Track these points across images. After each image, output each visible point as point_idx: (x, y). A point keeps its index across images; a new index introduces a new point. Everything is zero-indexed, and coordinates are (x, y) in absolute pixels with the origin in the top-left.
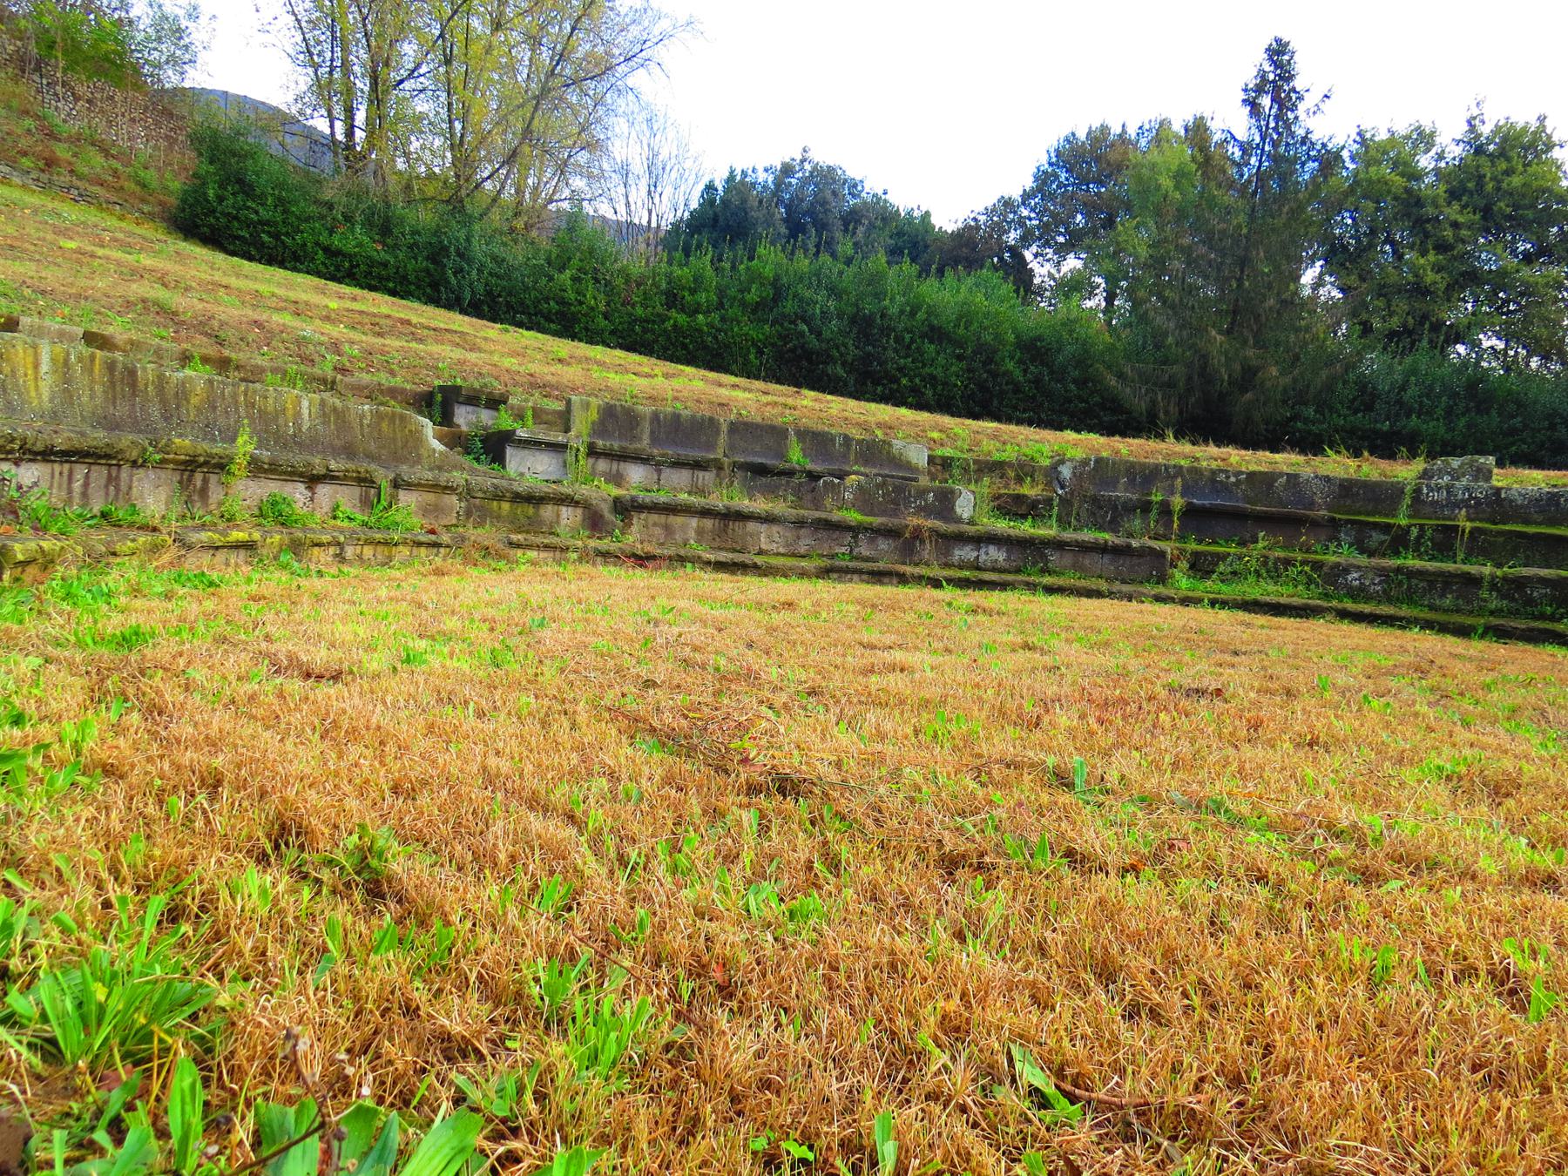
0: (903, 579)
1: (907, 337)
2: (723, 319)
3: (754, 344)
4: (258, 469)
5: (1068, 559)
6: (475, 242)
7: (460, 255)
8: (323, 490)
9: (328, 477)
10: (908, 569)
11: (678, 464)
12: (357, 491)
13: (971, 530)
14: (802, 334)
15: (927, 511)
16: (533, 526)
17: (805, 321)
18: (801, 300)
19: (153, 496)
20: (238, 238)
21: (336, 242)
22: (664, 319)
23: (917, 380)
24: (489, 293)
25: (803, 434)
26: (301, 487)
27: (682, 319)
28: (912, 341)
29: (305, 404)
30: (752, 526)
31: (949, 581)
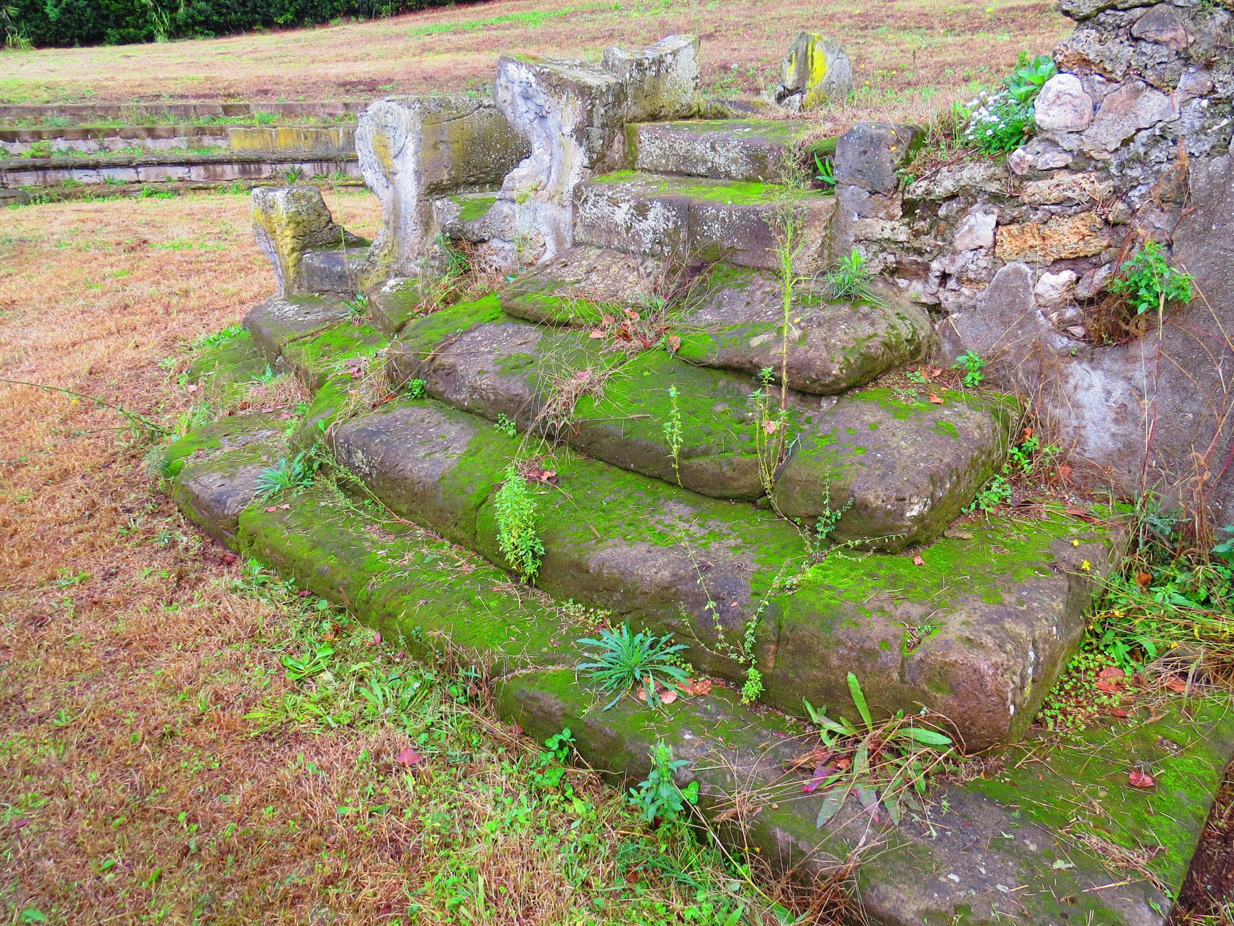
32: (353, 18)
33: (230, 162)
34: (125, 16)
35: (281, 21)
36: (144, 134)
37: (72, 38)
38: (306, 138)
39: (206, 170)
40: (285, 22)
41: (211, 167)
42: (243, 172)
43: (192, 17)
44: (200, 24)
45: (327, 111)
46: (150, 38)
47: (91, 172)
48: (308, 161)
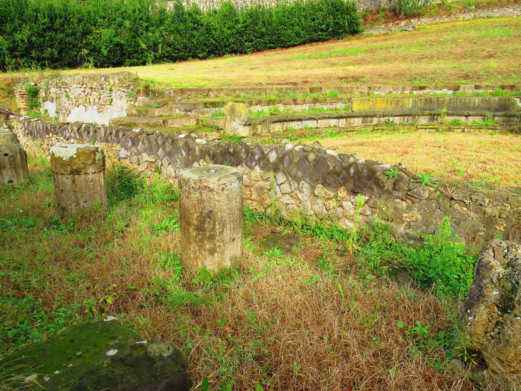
4: (448, 115)
9: (469, 115)
12: (481, 118)
19: (423, 120)
26: (464, 117)
29: (477, 100)
32: (233, 54)
33: (359, 117)
34: (133, 53)
35: (201, 55)
36: (292, 102)
37: (109, 64)
38: (391, 104)
39: (347, 121)
40: (203, 56)
41: (349, 119)
42: (363, 122)
43: (163, 54)
44: (166, 57)
45: (359, 90)
46: (144, 64)
47: (299, 123)
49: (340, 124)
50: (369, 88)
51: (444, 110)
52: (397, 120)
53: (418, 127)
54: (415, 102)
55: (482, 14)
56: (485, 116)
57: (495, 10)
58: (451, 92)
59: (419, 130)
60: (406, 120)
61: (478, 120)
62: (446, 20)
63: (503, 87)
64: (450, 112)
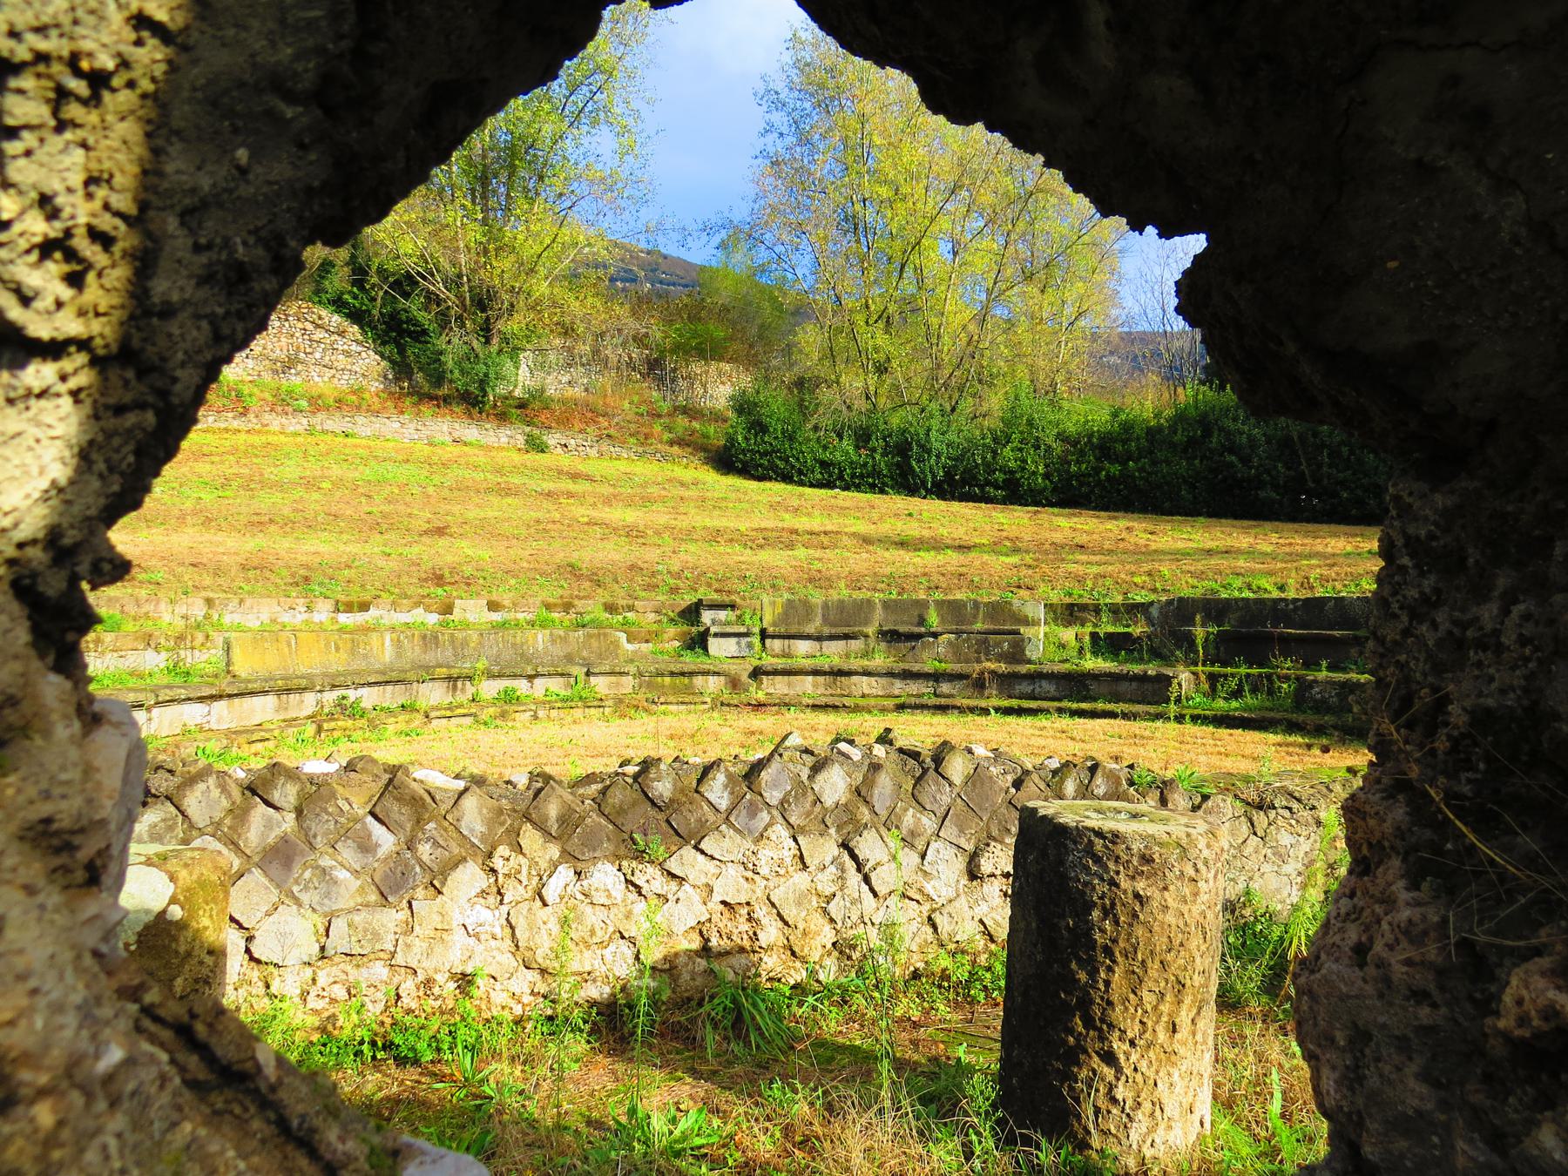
0: (962, 710)
1: (1345, 450)
2: (1154, 463)
3: (1185, 481)
4: (492, 676)
5: (1104, 689)
6: (933, 434)
7: (922, 446)
8: (537, 681)
9: (537, 675)
10: (966, 702)
11: (832, 638)
12: (561, 680)
13: (1023, 669)
14: (1231, 465)
15: (1001, 657)
16: (689, 690)
17: (1231, 451)
18: (1228, 433)
20: (761, 465)
21: (827, 456)
22: (1097, 470)
23: (1359, 492)
24: (947, 474)
25: (937, 602)
26: (524, 682)
27: (1115, 469)
28: (1352, 452)
30: (855, 678)
31: (997, 710)
38: (337, 649)
48: (370, 684)
49: (213, 719)
50: (209, 602)
51: (480, 666)
52: (368, 697)
53: (433, 714)
54: (398, 644)
55: (330, 425)
56: (569, 675)
57: (360, 420)
58: (433, 619)
59: (435, 722)
60: (388, 695)
61: (556, 685)
62: (235, 424)
63: (548, 607)
64: (496, 669)
